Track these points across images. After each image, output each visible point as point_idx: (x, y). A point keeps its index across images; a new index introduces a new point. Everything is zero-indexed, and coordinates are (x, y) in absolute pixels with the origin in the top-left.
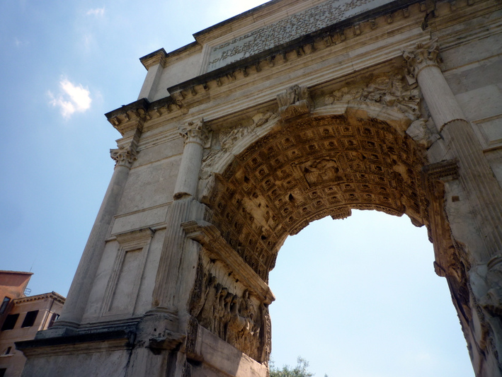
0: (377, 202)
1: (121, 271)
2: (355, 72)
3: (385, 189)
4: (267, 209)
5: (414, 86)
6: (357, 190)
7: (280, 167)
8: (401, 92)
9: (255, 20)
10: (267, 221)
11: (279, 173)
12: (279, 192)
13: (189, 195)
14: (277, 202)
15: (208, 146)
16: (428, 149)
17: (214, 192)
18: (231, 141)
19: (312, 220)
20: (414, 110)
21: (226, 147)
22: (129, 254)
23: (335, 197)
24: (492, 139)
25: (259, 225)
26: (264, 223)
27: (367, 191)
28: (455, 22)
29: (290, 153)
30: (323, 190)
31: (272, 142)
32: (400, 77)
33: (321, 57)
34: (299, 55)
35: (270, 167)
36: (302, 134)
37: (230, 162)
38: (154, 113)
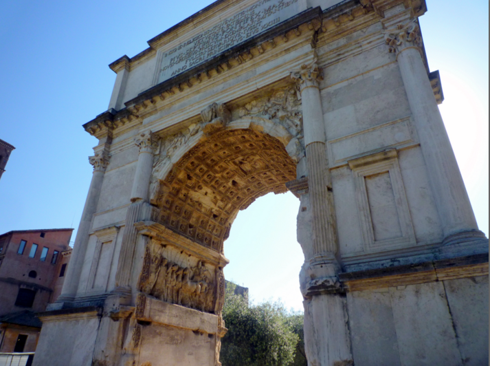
1: (99, 258)
2: (258, 89)
4: (214, 195)
7: (216, 164)
8: (292, 107)
9: (195, 26)
12: (221, 181)
13: (141, 199)
14: (221, 189)
15: (157, 152)
17: (160, 194)
19: (257, 196)
21: (170, 154)
25: (208, 208)
26: (213, 205)
28: (339, 36)
29: (221, 153)
31: (202, 149)
32: (293, 92)
33: (236, 74)
34: (218, 72)
35: (207, 165)
36: (226, 140)
37: (170, 170)
38: (118, 122)
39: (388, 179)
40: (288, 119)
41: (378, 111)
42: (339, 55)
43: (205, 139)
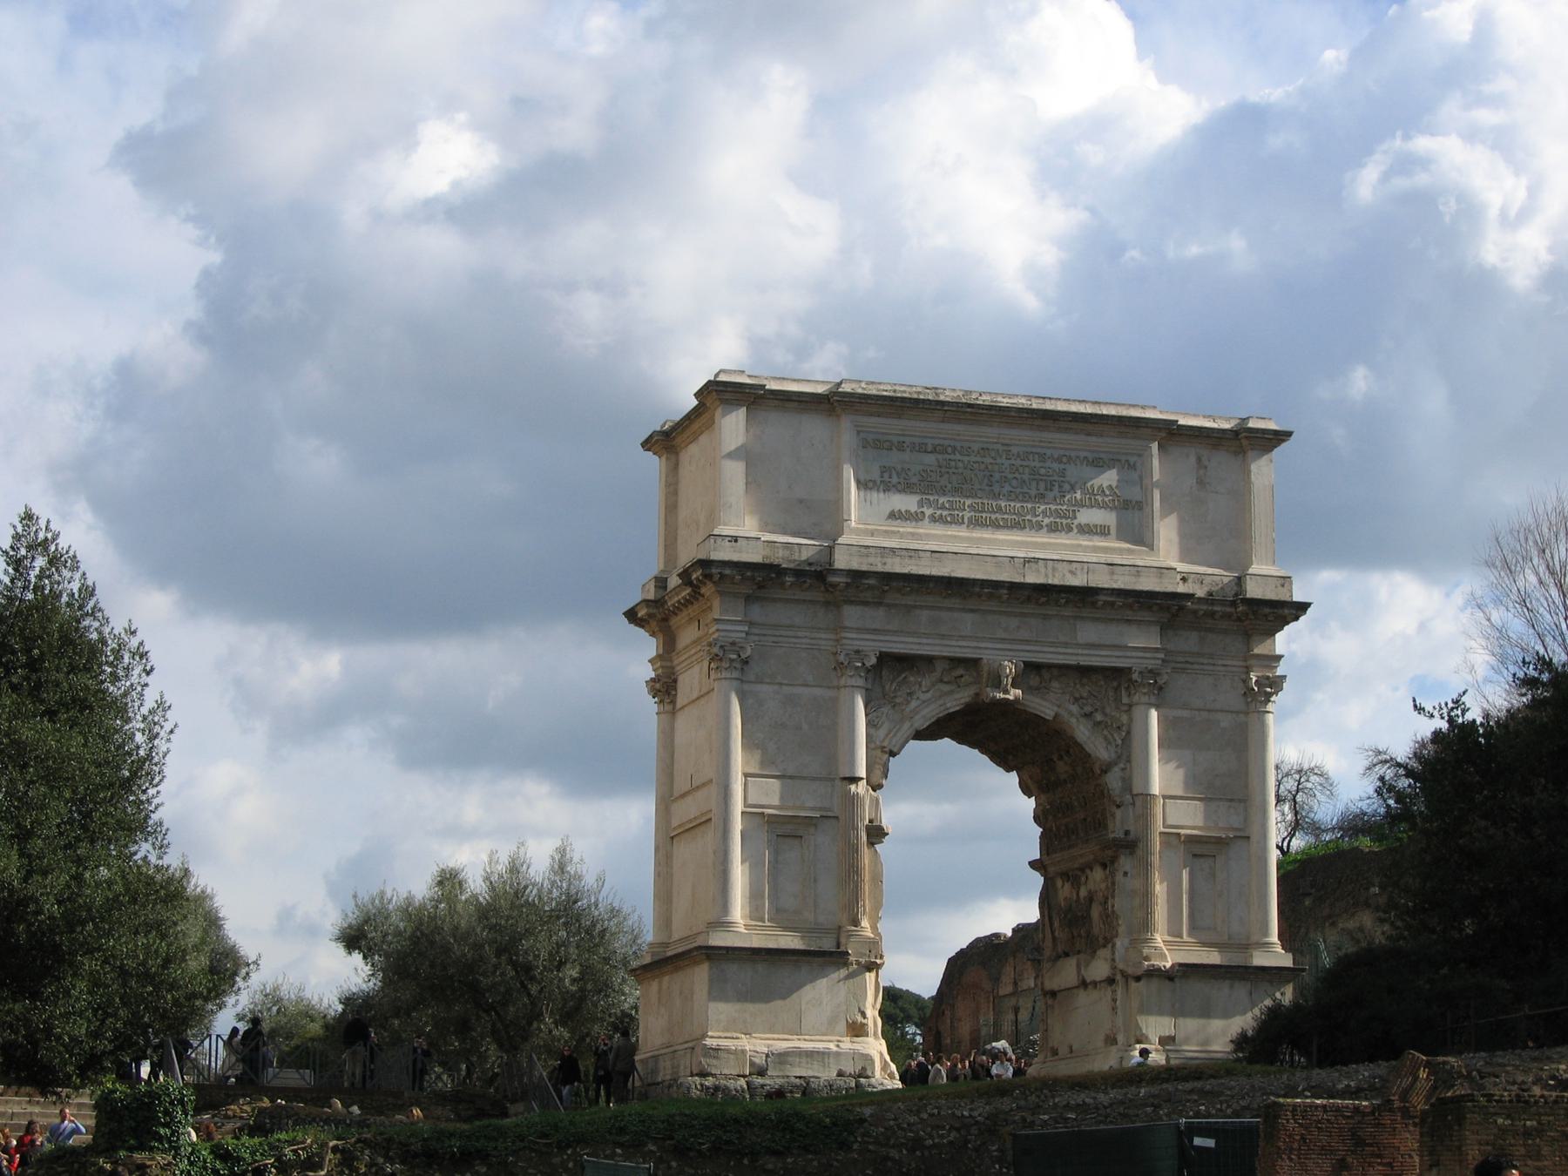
16: (1118, 806)
21: (897, 700)
24: (1169, 822)
32: (1115, 684)
41: (1217, 776)
42: (1187, 662)
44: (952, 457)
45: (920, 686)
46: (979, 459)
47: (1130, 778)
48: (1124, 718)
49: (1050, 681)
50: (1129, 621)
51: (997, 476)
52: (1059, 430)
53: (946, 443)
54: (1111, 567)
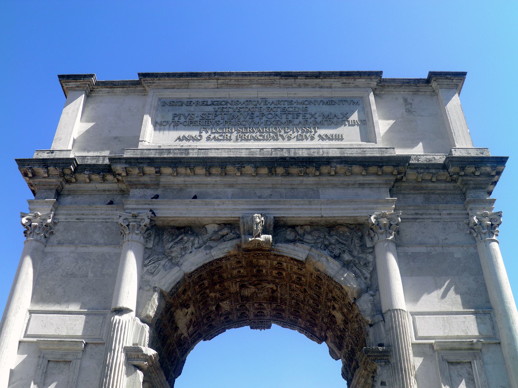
0: (302, 326)
3: (315, 320)
5: (371, 250)
6: (287, 312)
8: (358, 254)
10: (188, 329)
11: (218, 286)
16: (371, 325)
18: (179, 250)
20: (366, 278)
21: (173, 255)
22: (51, 365)
23: (262, 312)
24: (420, 334)
27: (296, 315)
30: (253, 305)
32: (360, 234)
36: (255, 260)
37: (178, 280)
39: (470, 370)
40: (355, 266)
42: (417, 214)
43: (236, 252)
44: (225, 106)
45: (193, 244)
46: (244, 106)
47: (380, 302)
48: (370, 258)
49: (304, 235)
50: (362, 185)
51: (257, 113)
52: (299, 86)
53: (221, 100)
54: (341, 150)
